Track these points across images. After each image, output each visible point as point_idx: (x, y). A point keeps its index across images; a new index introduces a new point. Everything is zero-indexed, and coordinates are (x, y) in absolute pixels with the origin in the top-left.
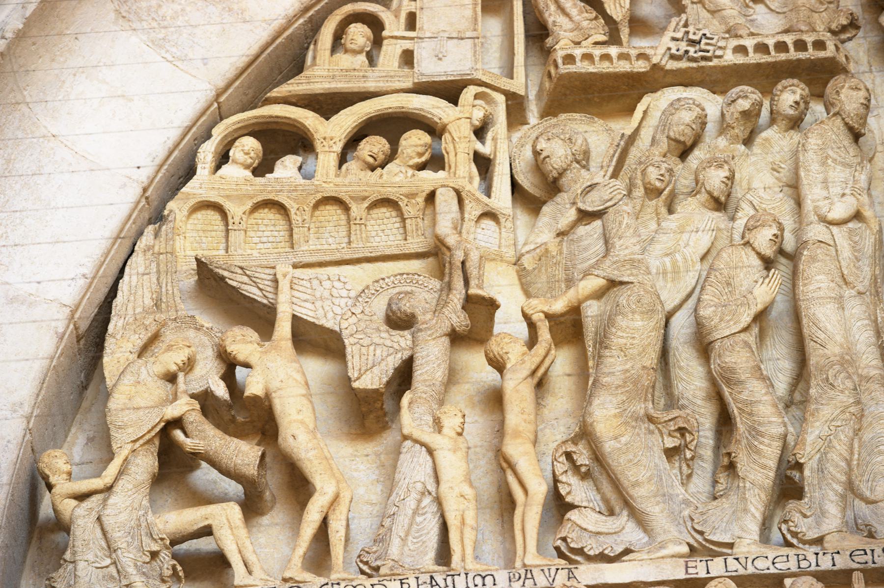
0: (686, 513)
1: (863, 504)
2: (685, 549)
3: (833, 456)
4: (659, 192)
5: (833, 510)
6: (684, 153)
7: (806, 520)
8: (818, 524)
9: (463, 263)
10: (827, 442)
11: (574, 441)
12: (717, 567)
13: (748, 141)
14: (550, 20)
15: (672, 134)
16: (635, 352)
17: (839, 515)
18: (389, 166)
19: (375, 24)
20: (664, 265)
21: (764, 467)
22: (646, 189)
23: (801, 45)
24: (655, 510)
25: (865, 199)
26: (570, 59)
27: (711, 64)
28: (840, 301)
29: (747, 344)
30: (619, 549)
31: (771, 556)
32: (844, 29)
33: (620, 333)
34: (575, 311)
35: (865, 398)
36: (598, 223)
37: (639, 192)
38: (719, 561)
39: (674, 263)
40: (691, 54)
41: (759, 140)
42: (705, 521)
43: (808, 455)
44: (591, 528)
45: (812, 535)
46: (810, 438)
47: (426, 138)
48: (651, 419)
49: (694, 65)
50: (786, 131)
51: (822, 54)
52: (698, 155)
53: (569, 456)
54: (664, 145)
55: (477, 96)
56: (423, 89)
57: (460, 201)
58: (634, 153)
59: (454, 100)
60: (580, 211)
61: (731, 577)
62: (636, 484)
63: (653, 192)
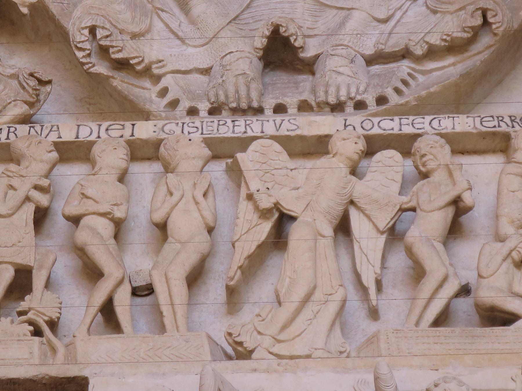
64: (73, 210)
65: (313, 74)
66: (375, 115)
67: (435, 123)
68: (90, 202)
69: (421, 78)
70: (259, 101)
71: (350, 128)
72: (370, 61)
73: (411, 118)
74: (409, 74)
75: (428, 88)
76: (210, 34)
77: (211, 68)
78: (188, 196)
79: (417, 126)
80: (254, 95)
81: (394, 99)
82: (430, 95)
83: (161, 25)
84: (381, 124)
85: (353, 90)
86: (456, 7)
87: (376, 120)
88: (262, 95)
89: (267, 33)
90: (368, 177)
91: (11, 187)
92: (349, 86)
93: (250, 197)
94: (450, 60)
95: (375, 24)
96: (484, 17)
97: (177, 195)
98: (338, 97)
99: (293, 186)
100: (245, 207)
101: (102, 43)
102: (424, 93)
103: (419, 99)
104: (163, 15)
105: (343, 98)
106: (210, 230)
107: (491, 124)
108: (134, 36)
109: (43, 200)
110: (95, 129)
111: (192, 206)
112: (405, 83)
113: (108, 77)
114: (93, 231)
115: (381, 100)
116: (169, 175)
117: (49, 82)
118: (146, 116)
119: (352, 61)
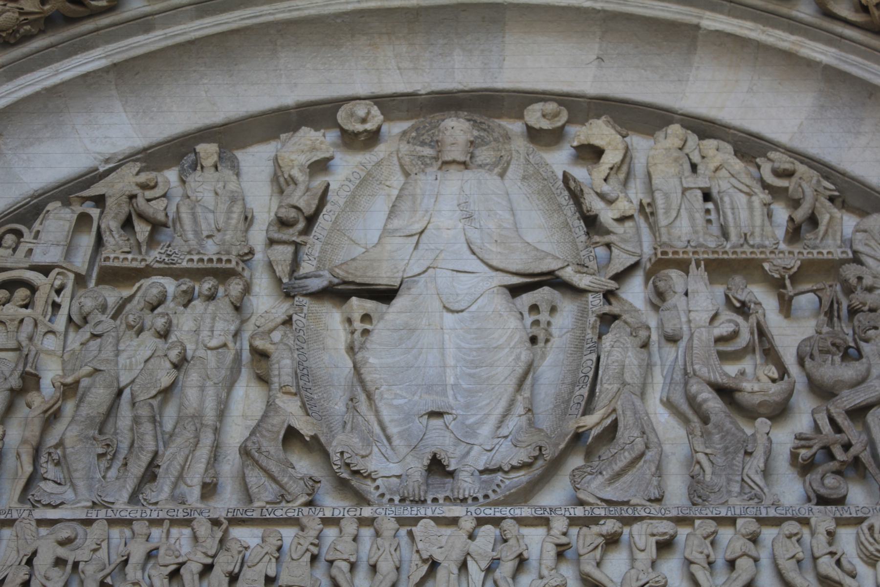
0: (97, 486)
1: (186, 487)
2: (90, 504)
3: (175, 463)
4: (133, 327)
5: (167, 489)
6: (153, 309)
7: (153, 493)
8: (158, 495)
9: (27, 355)
10: (174, 455)
11: (56, 447)
12: (102, 514)
13: (186, 306)
14: (105, 239)
15: (147, 299)
16: (96, 405)
17: (169, 492)
18: (7, 305)
19: (19, 234)
20: (126, 362)
21: (139, 466)
22: (127, 325)
23: (220, 260)
24: (81, 484)
25: (230, 338)
26: (107, 259)
27: (175, 266)
28: (202, 388)
29: (151, 406)
30: (58, 502)
31: (129, 510)
32: (246, 254)
33: (91, 395)
34: (77, 382)
35: (202, 436)
36: (99, 340)
37: (124, 326)
38: (104, 511)
39: (131, 363)
40: (166, 260)
41: (190, 305)
42: (104, 491)
43: (163, 462)
44: (48, 490)
45: (153, 501)
46: (167, 453)
47: (28, 292)
48: (94, 439)
49: (167, 266)
50: (205, 301)
51: (228, 266)
52: (159, 310)
53: (50, 454)
54: (142, 304)
55: (58, 274)
56: (33, 268)
57: (36, 325)
58: (128, 307)
59: (47, 275)
60: (92, 334)
61: (107, 520)
62: (76, 470)
63: (130, 327)
64: (330, 558)
65: (453, 478)
66: (482, 506)
67: (512, 511)
68: (338, 553)
69: (507, 482)
70: (424, 497)
71: (469, 513)
72: (482, 472)
73: (500, 508)
74: (501, 480)
75: (510, 490)
76: (401, 457)
77: (401, 475)
78: (387, 551)
79: (503, 513)
80: (422, 494)
81: (493, 496)
82: (511, 494)
83: (377, 450)
84: (485, 511)
85: (472, 491)
86: (527, 444)
87: (482, 509)
88: (426, 492)
89: (430, 458)
90: (478, 539)
91: (299, 544)
92: (470, 489)
93: (418, 551)
94: (522, 473)
95: (485, 452)
96: (540, 450)
97: (382, 550)
98: (464, 495)
99: (439, 545)
100: (416, 557)
101: (347, 461)
102: (508, 493)
103: (506, 497)
104: (378, 444)
105: (466, 496)
106: (398, 569)
107: (540, 512)
108: (363, 457)
109: (315, 550)
110: (342, 510)
111: (389, 557)
112: (498, 486)
113: (349, 480)
114: (339, 568)
115: (486, 496)
116: (379, 539)
117: (320, 482)
118: (369, 503)
119: (472, 475)
